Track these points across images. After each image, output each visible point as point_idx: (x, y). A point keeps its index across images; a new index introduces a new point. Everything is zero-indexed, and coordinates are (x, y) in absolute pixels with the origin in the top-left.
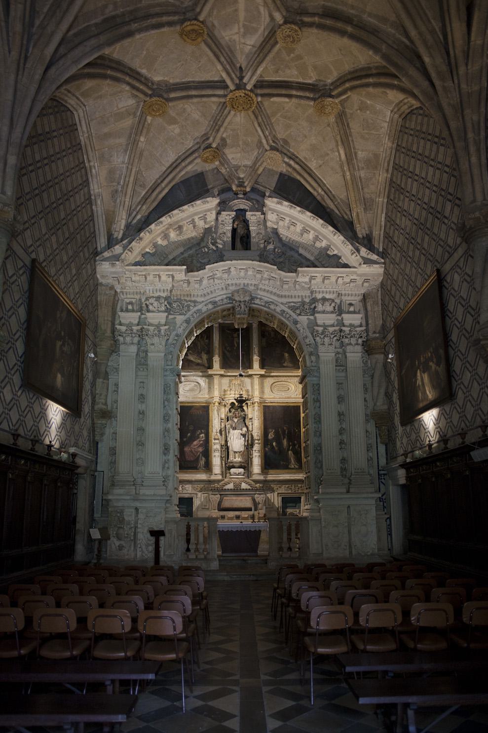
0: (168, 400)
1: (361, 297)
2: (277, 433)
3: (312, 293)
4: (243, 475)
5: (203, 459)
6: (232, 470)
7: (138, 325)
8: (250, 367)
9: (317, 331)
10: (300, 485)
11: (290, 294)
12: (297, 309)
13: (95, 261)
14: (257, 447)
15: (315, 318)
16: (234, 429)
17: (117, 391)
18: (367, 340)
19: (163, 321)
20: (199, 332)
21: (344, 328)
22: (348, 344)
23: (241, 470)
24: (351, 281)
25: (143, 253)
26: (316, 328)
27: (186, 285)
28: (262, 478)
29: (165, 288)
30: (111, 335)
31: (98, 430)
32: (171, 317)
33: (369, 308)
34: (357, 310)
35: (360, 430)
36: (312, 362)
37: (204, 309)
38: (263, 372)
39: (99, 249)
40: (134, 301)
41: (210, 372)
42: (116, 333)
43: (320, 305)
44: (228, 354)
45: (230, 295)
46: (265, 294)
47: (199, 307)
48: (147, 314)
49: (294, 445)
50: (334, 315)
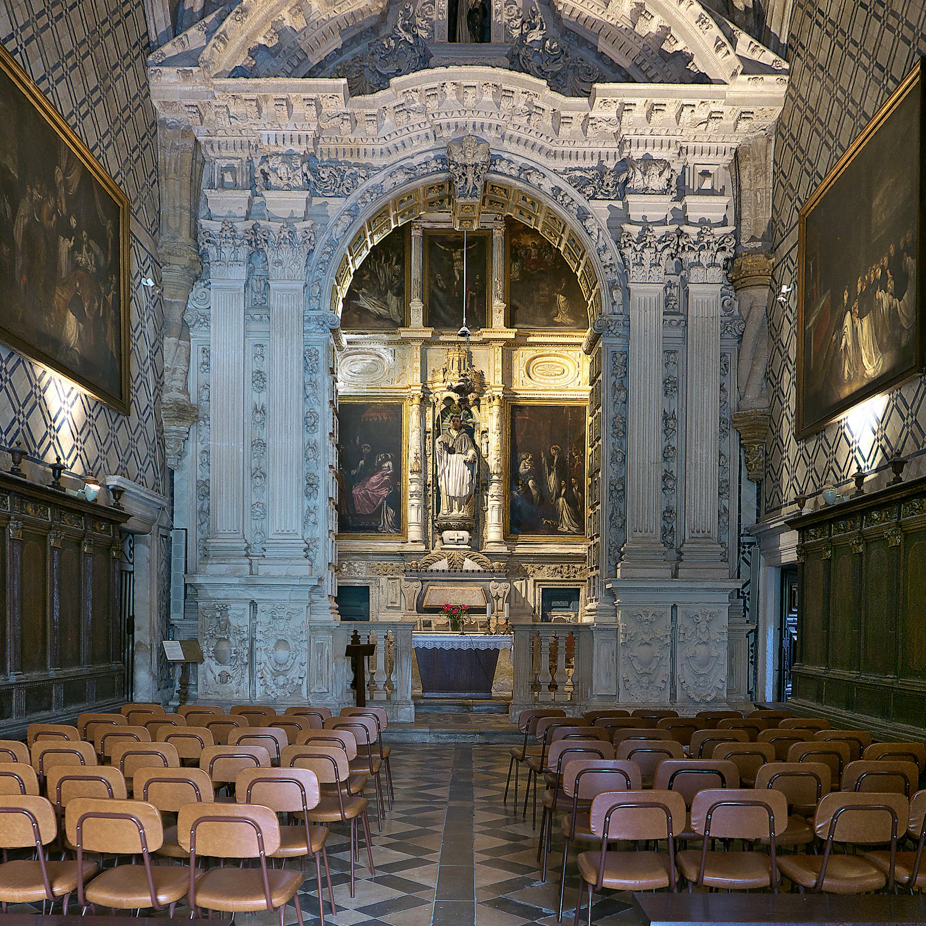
0: (313, 384)
1: (730, 157)
2: (536, 462)
3: (622, 145)
7: (247, 219)
9: (629, 234)
10: (578, 566)
11: (574, 150)
12: (589, 182)
13: (146, 65)
15: (626, 205)
16: (451, 451)
17: (208, 365)
18: (736, 256)
19: (300, 211)
20: (377, 239)
21: (686, 229)
22: (692, 265)
23: (465, 534)
24: (710, 117)
25: (252, 46)
26: (627, 227)
27: (346, 126)
28: (504, 549)
29: (303, 133)
30: (191, 241)
31: (170, 445)
32: (316, 201)
33: (745, 183)
34: (718, 188)
35: (706, 449)
36: (614, 303)
37: (388, 184)
39: (153, 38)
40: (236, 163)
41: (404, 333)
42: (201, 236)
43: (639, 175)
44: (440, 294)
45: (442, 152)
46: (520, 149)
47: (377, 179)
48: (265, 193)
49: (570, 486)
50: (667, 199)
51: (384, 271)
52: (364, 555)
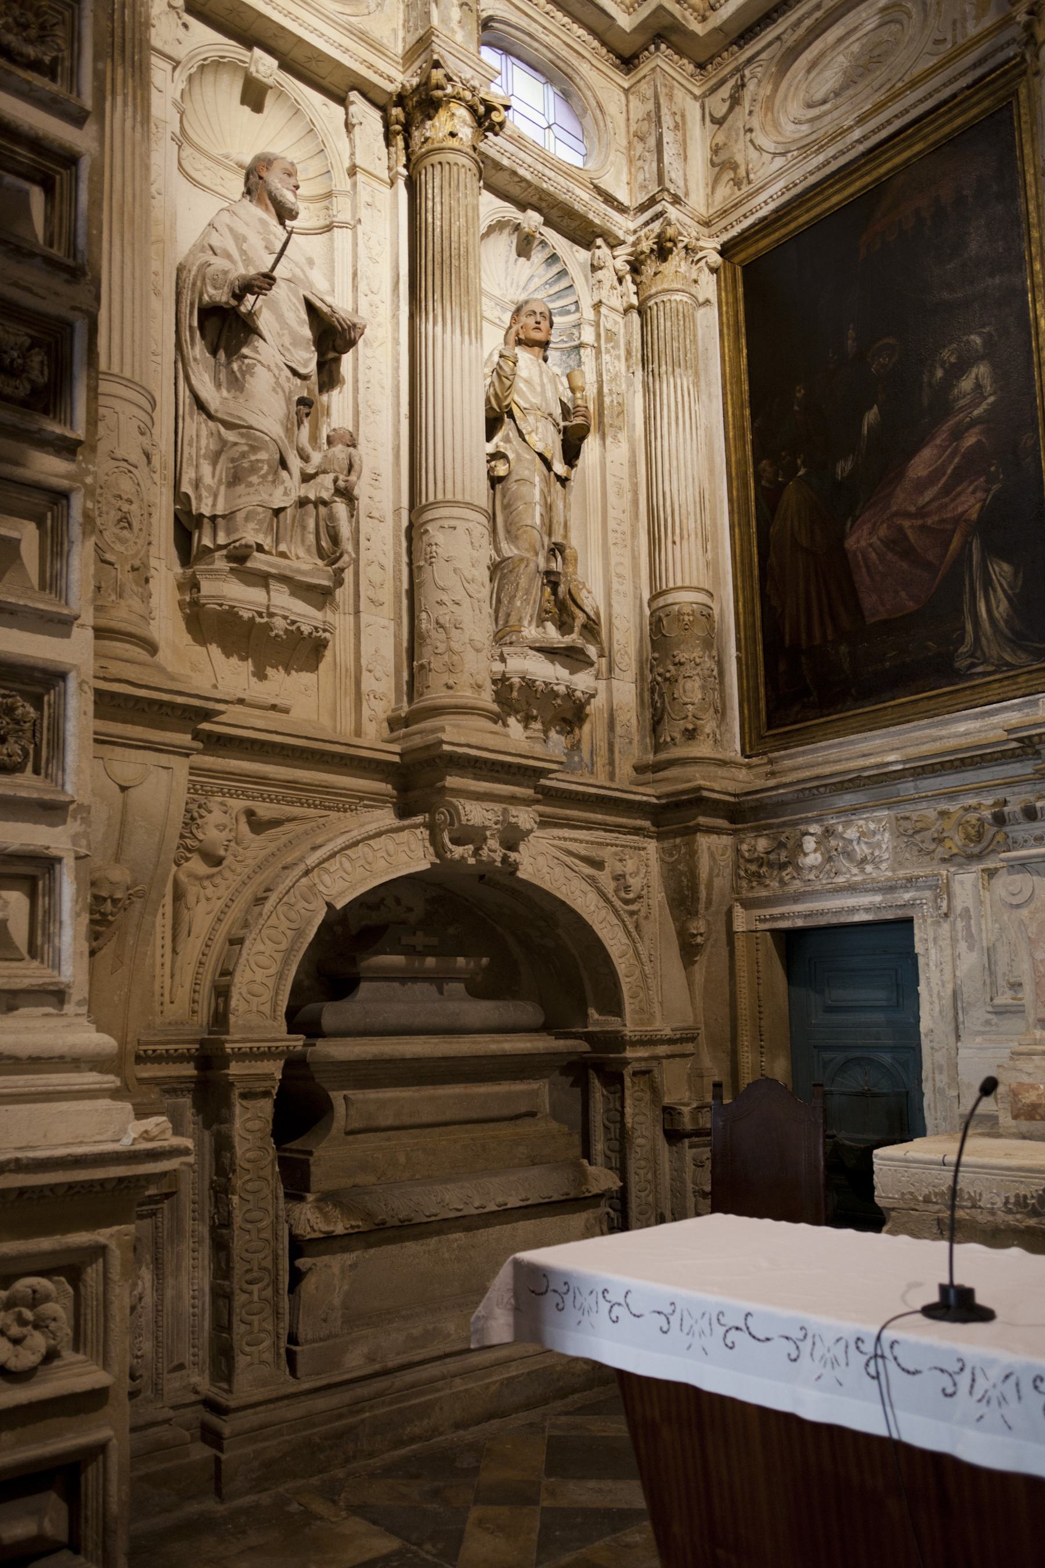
52: (875, 783)
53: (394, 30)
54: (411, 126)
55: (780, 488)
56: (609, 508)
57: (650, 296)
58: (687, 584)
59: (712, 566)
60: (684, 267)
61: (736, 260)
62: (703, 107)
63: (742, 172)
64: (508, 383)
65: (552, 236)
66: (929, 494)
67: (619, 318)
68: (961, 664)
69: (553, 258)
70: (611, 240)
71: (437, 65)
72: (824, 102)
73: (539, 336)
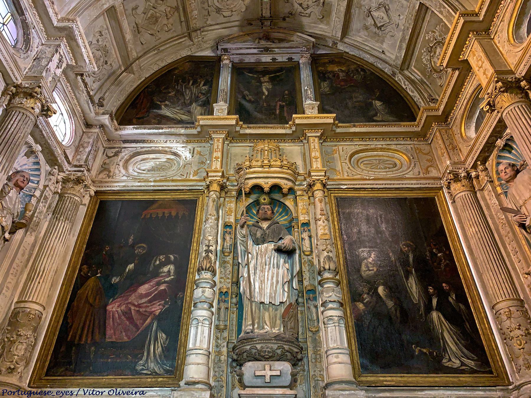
4: (291, 387)
5: (162, 336)
6: (250, 369)
8: (295, 106)
14: (331, 293)
38: (329, 118)
49: (442, 295)
51: (191, 90)
53: (25, 68)
54: (17, 95)
55: (89, 277)
56: (17, 259)
57: (67, 193)
58: (37, 301)
59: (50, 297)
60: (82, 190)
61: (99, 197)
62: (105, 150)
63: (111, 174)
64: (4, 195)
65: (41, 156)
66: (144, 300)
67: (51, 194)
68: (139, 368)
69: (38, 163)
70: (60, 169)
71: (40, 87)
72: (144, 171)
73: (22, 185)
